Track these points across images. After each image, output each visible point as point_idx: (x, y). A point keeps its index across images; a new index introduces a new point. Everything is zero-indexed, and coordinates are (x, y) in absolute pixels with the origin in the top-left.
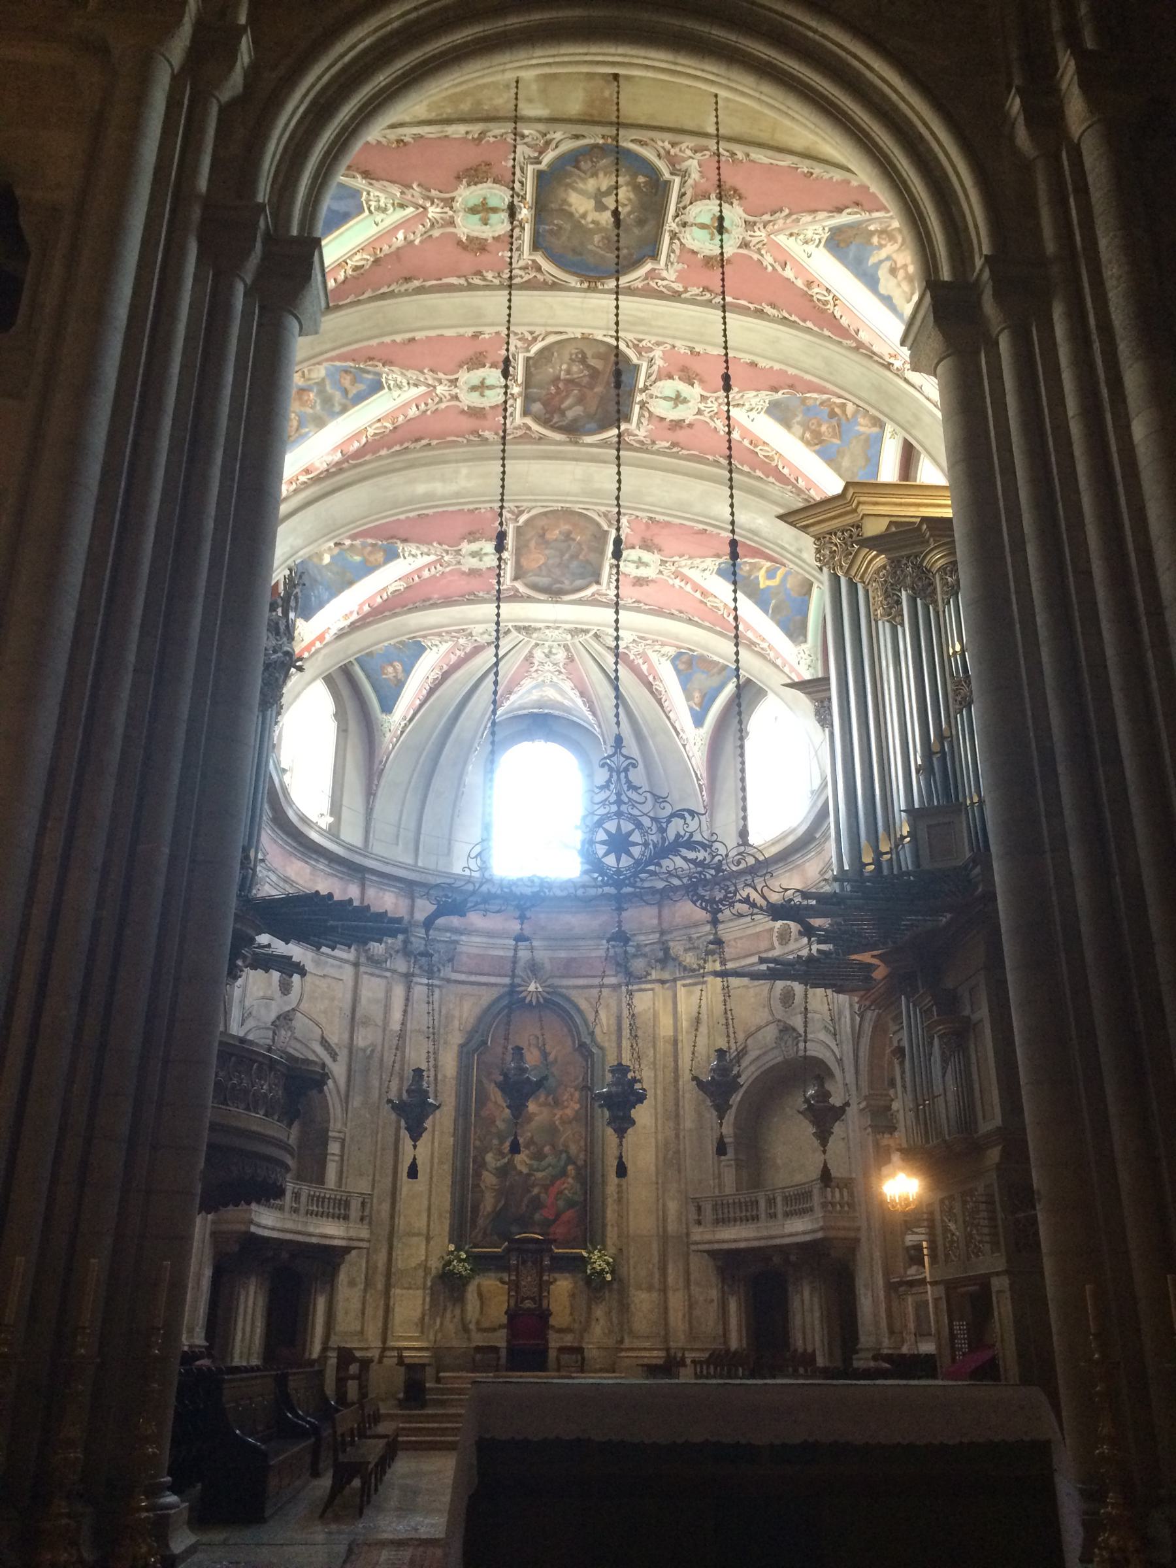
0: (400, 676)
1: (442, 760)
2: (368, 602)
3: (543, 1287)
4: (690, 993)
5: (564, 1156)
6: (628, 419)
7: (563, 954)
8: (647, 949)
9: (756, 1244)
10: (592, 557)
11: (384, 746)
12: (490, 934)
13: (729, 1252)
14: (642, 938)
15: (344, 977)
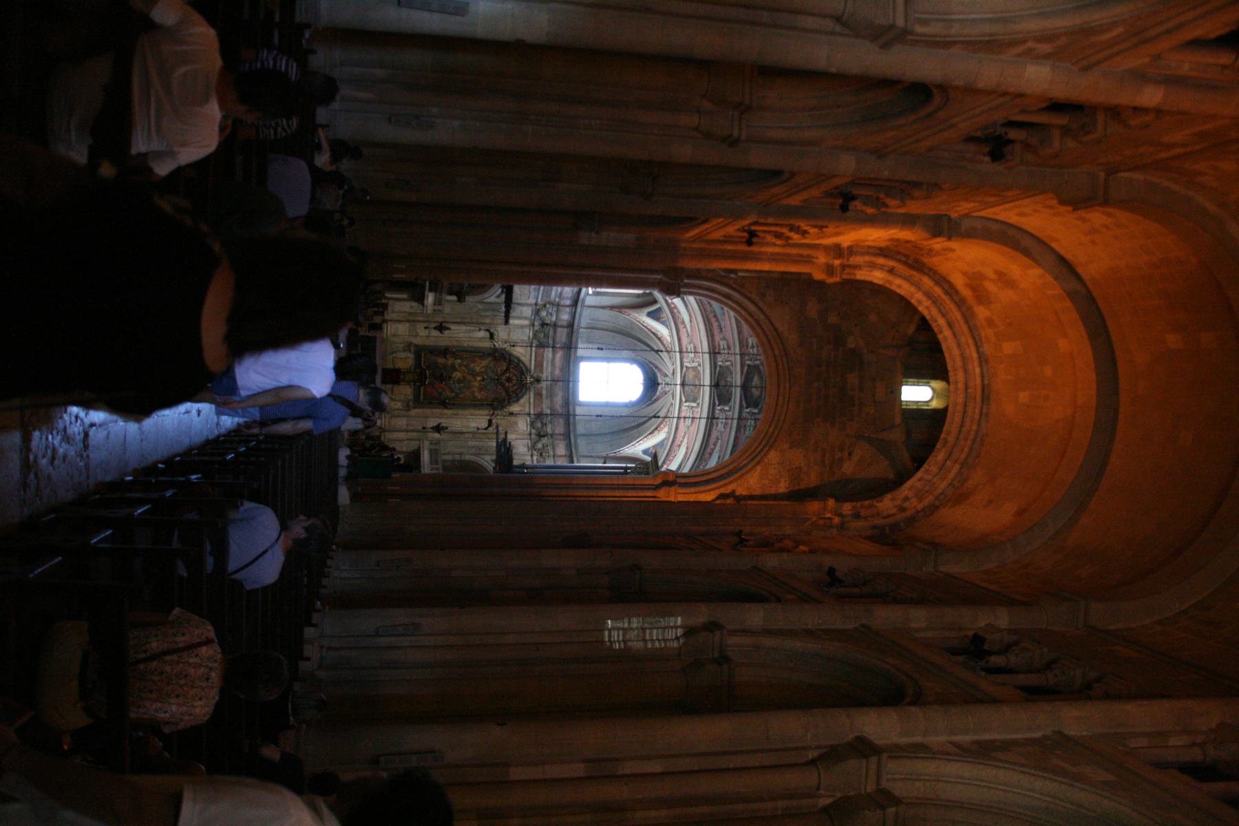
0: (661, 320)
1: (628, 339)
2: (676, 307)
3: (408, 383)
4: (524, 445)
5: (459, 392)
6: (719, 405)
7: (544, 392)
8: (544, 428)
9: (422, 463)
10: (691, 398)
11: (633, 314)
12: (553, 359)
13: (420, 454)
14: (550, 426)
15: (530, 299)
